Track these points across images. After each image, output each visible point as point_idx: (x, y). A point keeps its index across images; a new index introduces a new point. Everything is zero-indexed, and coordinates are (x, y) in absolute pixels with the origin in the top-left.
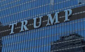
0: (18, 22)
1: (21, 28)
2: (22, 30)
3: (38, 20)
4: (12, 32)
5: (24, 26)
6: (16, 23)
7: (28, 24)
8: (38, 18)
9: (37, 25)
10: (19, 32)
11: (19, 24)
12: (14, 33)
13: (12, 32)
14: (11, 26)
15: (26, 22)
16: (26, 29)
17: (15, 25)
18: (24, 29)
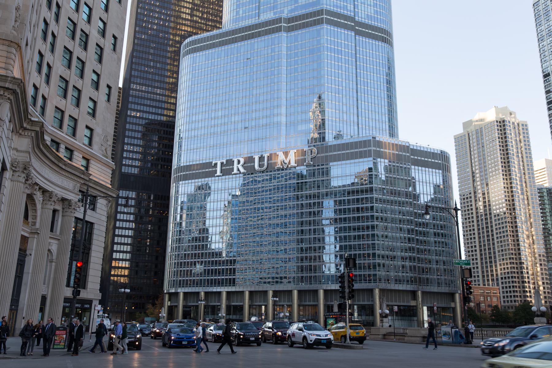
0: (228, 158)
1: (233, 168)
2: (235, 171)
3: (261, 158)
4: (218, 173)
5: (238, 166)
6: (224, 161)
7: (245, 163)
8: (262, 156)
9: (260, 166)
10: (230, 174)
11: (230, 162)
12: (223, 176)
13: (218, 173)
14: (216, 164)
15: (242, 161)
16: (242, 170)
17: (222, 163)
18: (238, 170)
